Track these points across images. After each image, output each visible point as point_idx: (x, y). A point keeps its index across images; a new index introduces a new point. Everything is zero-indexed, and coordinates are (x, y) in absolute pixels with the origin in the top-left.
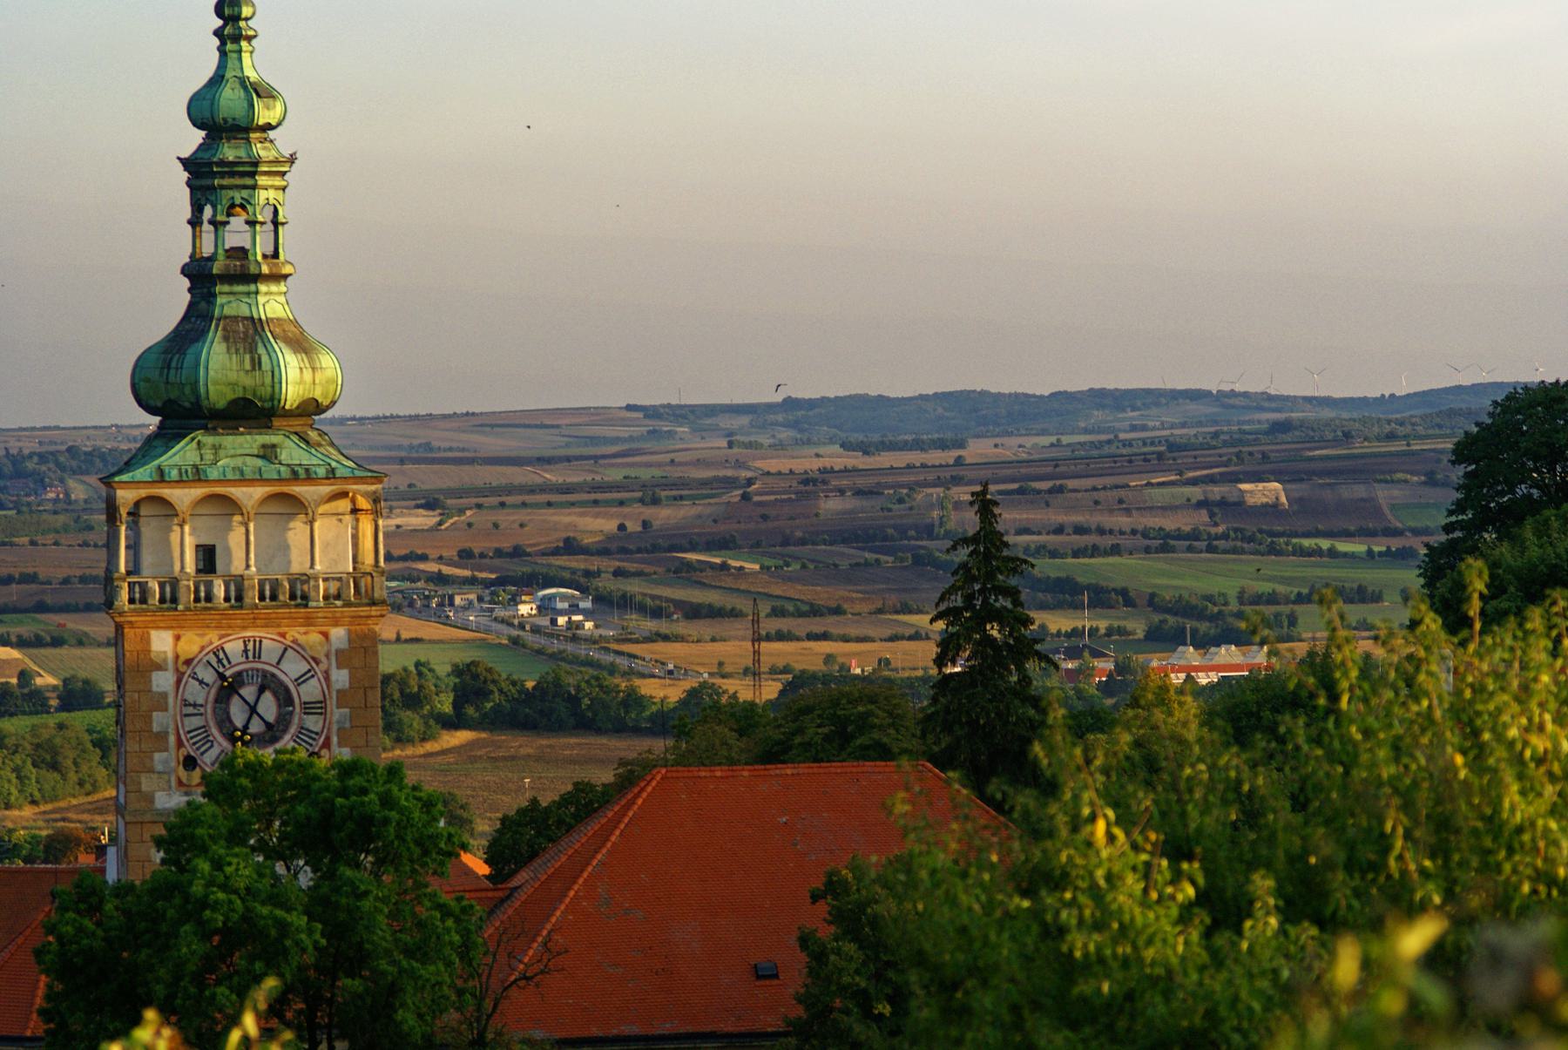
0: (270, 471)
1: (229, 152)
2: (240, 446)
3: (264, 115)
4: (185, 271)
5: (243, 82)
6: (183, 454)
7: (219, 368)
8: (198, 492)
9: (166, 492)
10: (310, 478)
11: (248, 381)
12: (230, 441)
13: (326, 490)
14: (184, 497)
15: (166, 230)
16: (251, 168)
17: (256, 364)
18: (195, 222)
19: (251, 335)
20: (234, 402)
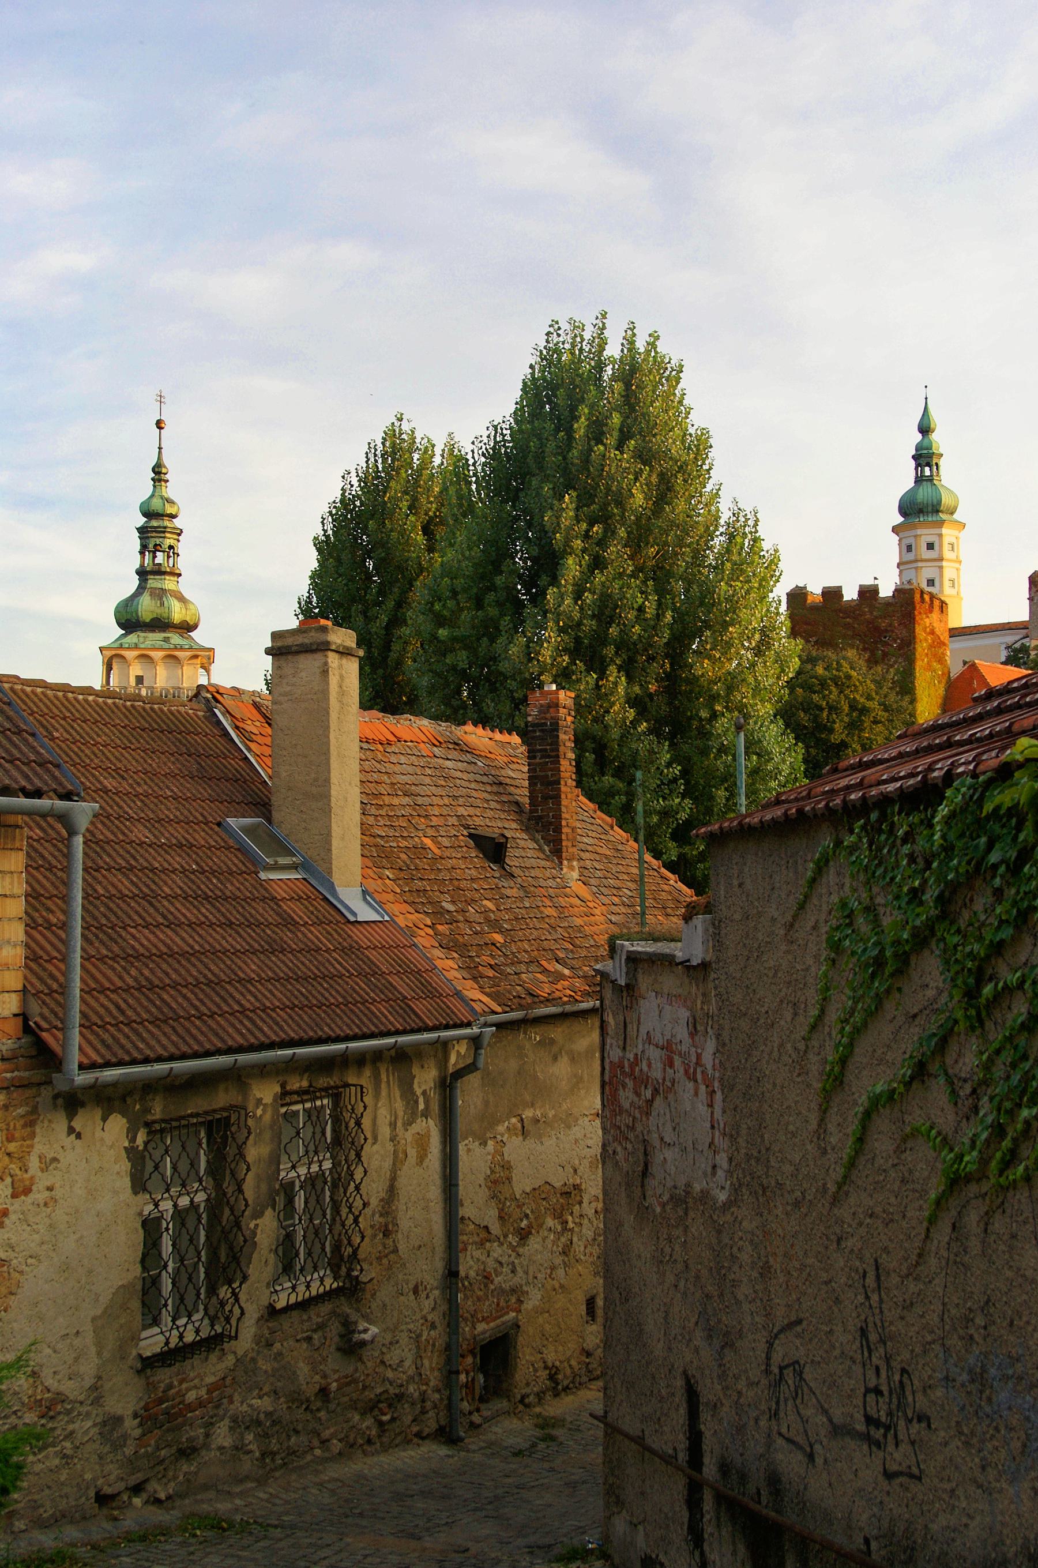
0: (166, 646)
1: (154, 523)
2: (155, 638)
3: (170, 510)
4: (138, 572)
5: (162, 497)
6: (132, 638)
7: (147, 607)
8: (136, 653)
9: (123, 653)
10: (182, 649)
11: (159, 611)
12: (151, 635)
13: (189, 654)
14: (130, 655)
15: (130, 557)
16: (162, 531)
17: (162, 604)
18: (142, 553)
19: (160, 594)
20: (153, 620)
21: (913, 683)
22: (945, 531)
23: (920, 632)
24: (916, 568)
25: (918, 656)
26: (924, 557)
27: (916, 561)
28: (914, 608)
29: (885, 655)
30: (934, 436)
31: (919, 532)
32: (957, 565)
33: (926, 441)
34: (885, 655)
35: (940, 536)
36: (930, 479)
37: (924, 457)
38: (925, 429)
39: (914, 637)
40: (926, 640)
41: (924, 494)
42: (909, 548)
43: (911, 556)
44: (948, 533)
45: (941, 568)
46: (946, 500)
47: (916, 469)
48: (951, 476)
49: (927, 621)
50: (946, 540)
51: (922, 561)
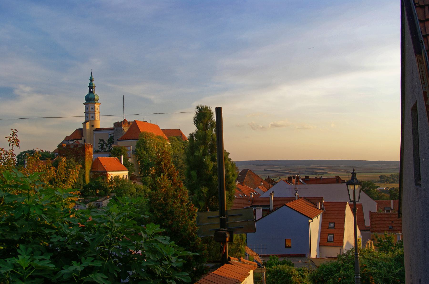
22: (96, 105)
23: (86, 153)
29: (79, 158)
30: (93, 82)
34: (79, 158)
36: (92, 92)
37: (91, 87)
38: (91, 80)
41: (91, 96)
42: (87, 108)
43: (88, 111)
44: (97, 106)
46: (96, 98)
48: (97, 93)
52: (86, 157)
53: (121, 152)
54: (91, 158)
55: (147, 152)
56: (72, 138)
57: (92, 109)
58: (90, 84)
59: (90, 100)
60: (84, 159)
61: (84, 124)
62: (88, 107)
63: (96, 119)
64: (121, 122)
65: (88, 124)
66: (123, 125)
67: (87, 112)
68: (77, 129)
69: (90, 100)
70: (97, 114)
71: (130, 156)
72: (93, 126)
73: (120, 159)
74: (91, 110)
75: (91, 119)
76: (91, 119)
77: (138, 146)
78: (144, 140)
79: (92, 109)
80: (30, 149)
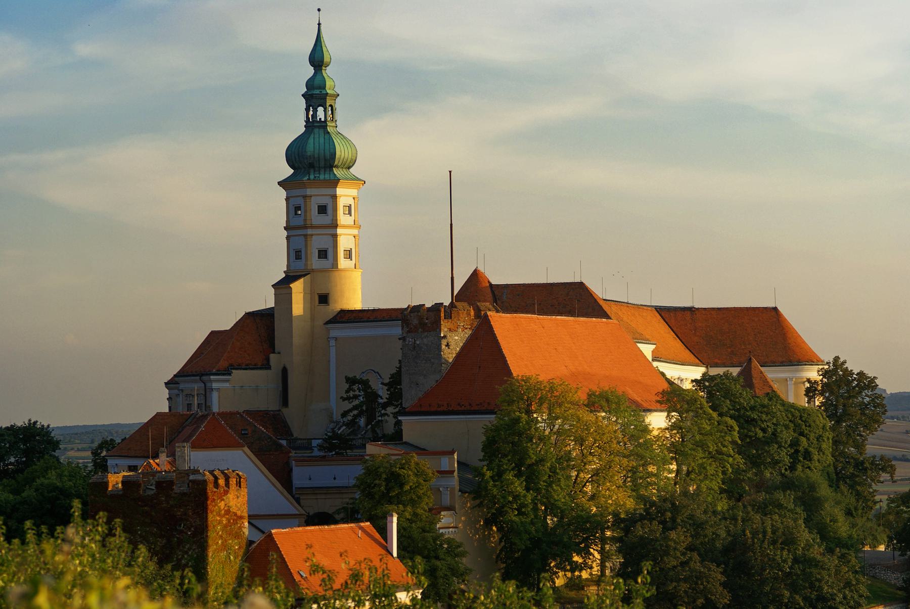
21: (205, 569)
22: (339, 191)
24: (306, 236)
25: (210, 542)
26: (314, 223)
27: (305, 227)
28: (207, 498)
30: (328, 72)
31: (309, 192)
32: (355, 232)
33: (318, 78)
35: (334, 197)
36: (323, 125)
37: (316, 95)
39: (207, 526)
40: (220, 522)
43: (299, 221)
44: (345, 194)
45: (335, 236)
46: (341, 152)
47: (307, 110)
49: (222, 505)
50: (342, 202)
51: (312, 227)
52: (211, 534)
53: (402, 485)
54: (238, 536)
55: (531, 478)
56: (223, 364)
57: (322, 209)
58: (310, 84)
59: (313, 165)
60: (203, 547)
61: (282, 287)
62: (300, 201)
63: (343, 263)
64: (437, 307)
65: (298, 287)
66: (445, 326)
67: (297, 227)
68: (249, 315)
69: (311, 166)
70: (345, 240)
71: (447, 501)
72: (324, 299)
73: (384, 531)
74: (316, 218)
75: (315, 263)
76: (315, 263)
77: (491, 448)
78: (517, 420)
79: (322, 209)
80: (20, 421)
